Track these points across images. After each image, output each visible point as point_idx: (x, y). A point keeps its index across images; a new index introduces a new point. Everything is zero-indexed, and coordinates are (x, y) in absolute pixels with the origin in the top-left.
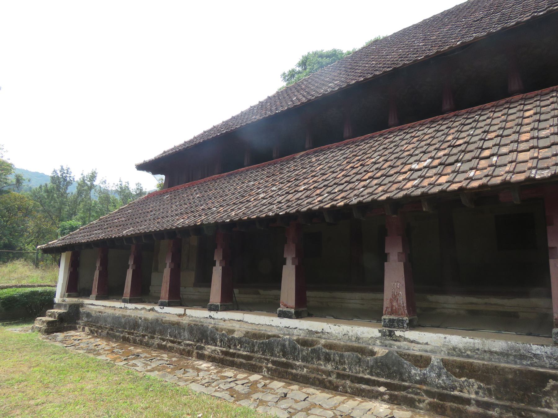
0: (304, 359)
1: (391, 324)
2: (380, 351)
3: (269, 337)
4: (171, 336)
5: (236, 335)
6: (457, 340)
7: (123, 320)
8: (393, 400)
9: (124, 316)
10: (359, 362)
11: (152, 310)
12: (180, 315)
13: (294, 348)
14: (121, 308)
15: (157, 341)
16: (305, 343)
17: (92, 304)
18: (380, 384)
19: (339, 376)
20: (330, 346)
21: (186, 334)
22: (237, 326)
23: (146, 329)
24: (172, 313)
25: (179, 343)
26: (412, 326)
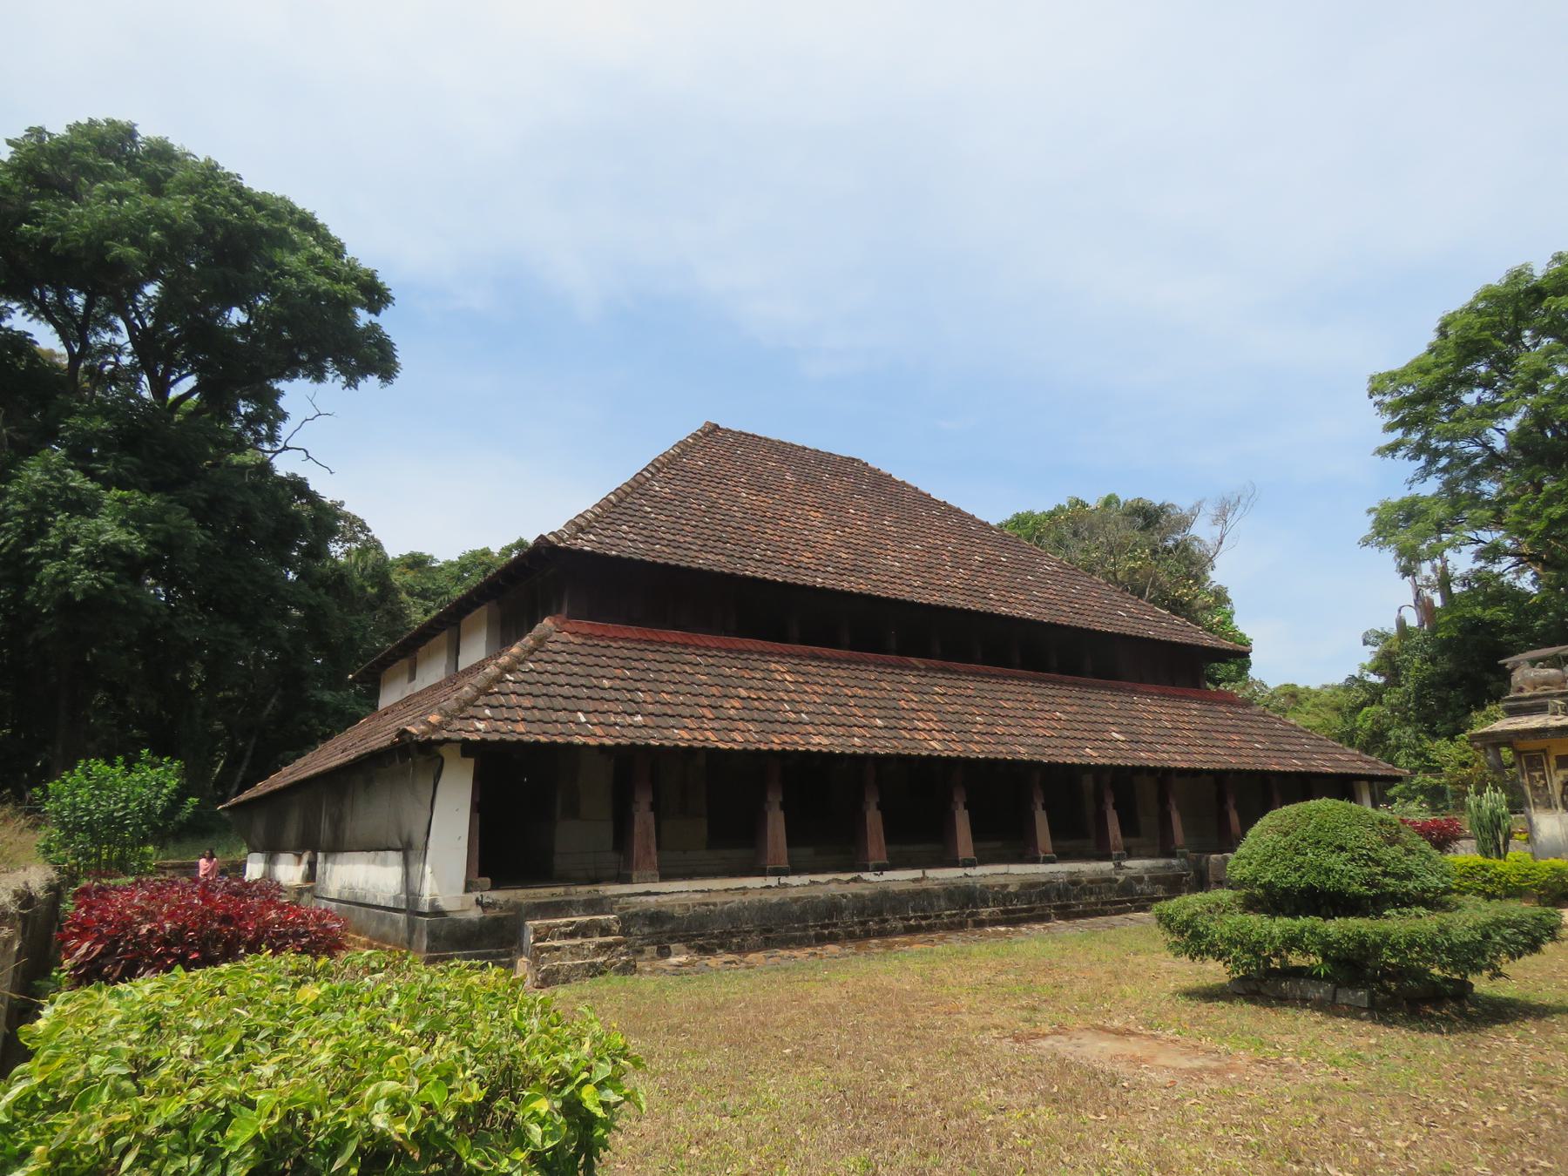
0: (1076, 898)
1: (1120, 857)
2: (1121, 878)
3: (1044, 884)
4: (914, 911)
5: (1011, 889)
6: (1148, 863)
7: (795, 907)
8: (1138, 910)
9: (796, 900)
10: (1110, 889)
11: (855, 880)
12: (915, 880)
13: (1067, 889)
14: (769, 887)
15: (900, 925)
16: (1075, 883)
17: (648, 893)
18: (1124, 902)
19: (1104, 904)
20: (1091, 882)
21: (943, 903)
22: (1002, 880)
23: (861, 912)
24: (901, 878)
25: (938, 916)
26: (1130, 857)
